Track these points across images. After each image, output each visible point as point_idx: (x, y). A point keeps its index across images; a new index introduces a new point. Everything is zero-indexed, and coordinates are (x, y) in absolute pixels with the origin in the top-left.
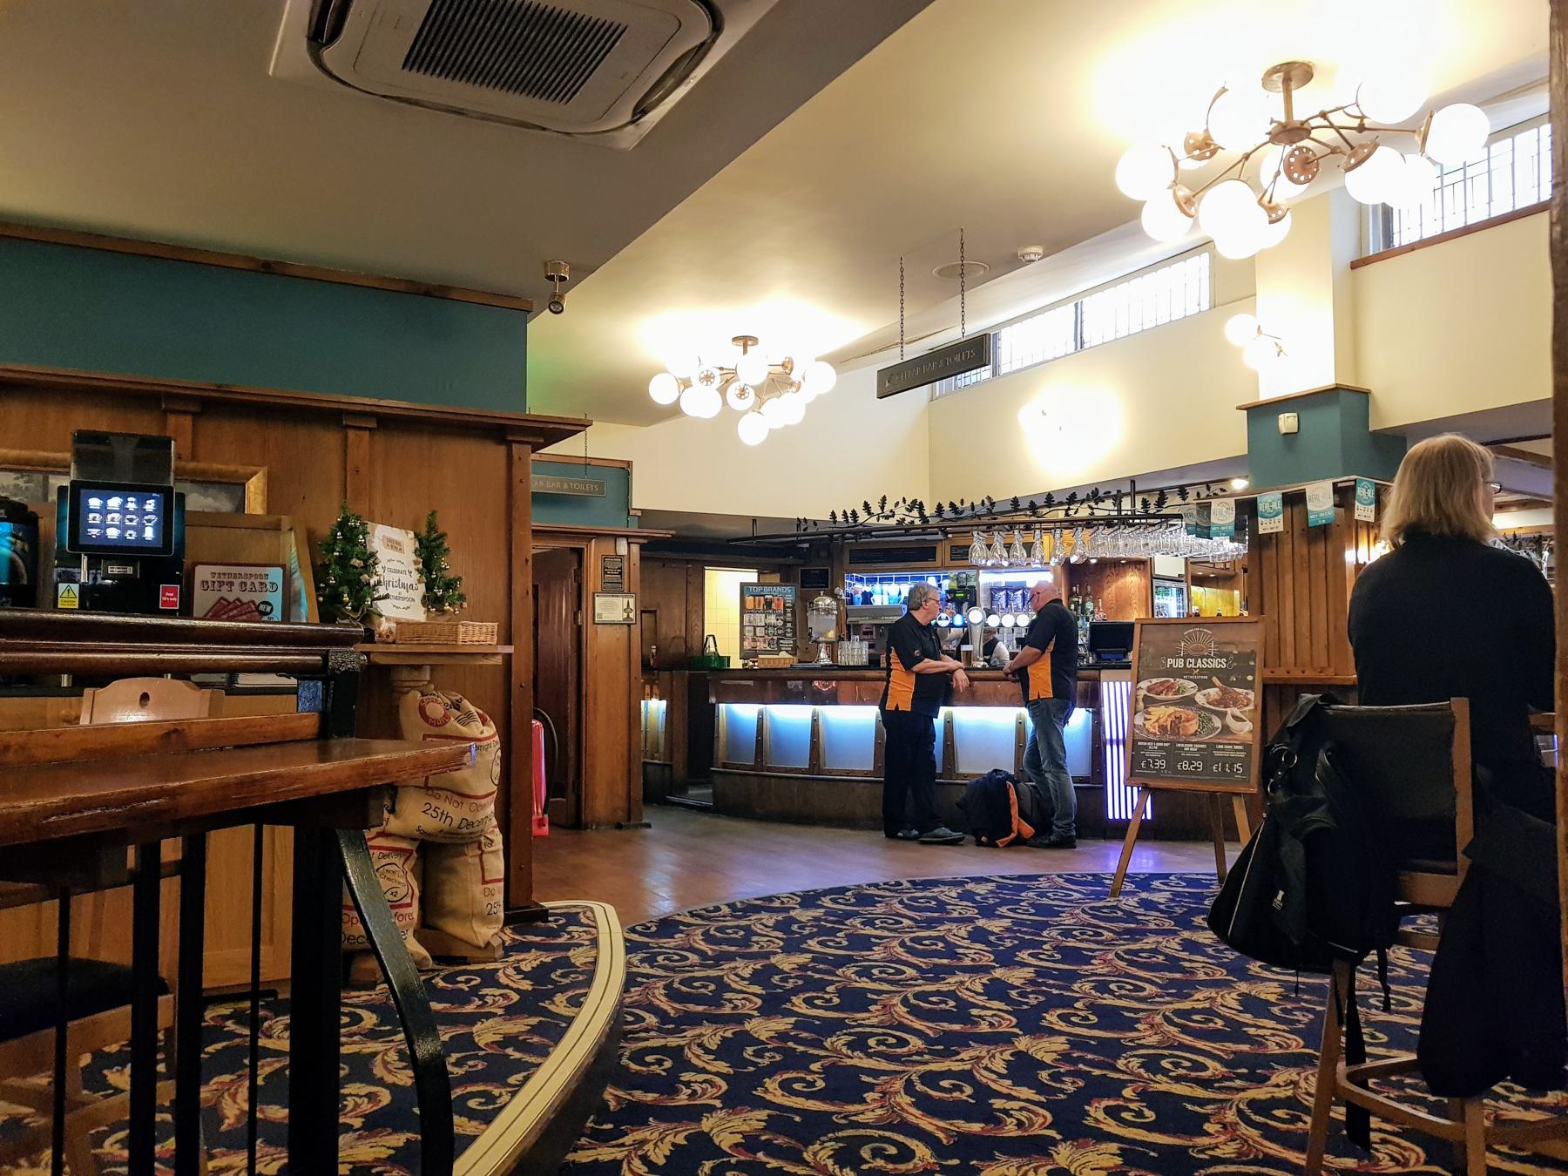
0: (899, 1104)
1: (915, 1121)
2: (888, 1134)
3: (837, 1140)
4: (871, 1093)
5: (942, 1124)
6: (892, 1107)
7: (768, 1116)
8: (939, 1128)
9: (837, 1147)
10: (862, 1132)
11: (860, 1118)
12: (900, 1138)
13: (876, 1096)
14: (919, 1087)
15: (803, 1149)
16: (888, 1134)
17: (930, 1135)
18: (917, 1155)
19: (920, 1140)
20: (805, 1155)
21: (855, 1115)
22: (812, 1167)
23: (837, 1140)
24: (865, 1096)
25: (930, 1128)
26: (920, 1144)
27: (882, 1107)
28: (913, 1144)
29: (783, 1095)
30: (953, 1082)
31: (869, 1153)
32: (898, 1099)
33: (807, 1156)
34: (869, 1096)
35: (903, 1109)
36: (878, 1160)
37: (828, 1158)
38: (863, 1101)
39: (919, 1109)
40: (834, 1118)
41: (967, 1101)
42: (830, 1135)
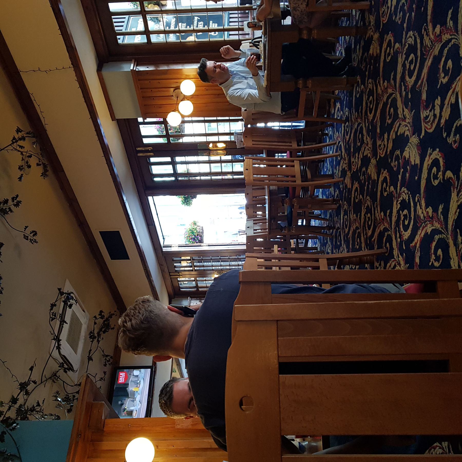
0: (426, 226)
1: (419, 233)
2: (412, 221)
3: (409, 199)
4: (432, 210)
5: (418, 245)
6: (425, 222)
7: (417, 164)
8: (416, 243)
9: (406, 200)
10: (412, 209)
11: (418, 207)
12: (411, 227)
13: (430, 214)
14: (437, 237)
15: (405, 186)
16: (412, 221)
17: (413, 240)
18: (405, 233)
19: (411, 234)
20: (403, 188)
21: (420, 205)
22: (399, 192)
23: (409, 199)
24: (430, 207)
25: (416, 240)
26: (409, 234)
27: (424, 217)
28: (409, 231)
29: (428, 165)
30: (441, 257)
31: (405, 213)
32: (429, 225)
33: (403, 189)
34: (430, 210)
35: (423, 228)
36: (403, 217)
37: (403, 197)
38: (427, 207)
39: (424, 235)
40: (418, 195)
41: (430, 261)
42: (411, 196)
